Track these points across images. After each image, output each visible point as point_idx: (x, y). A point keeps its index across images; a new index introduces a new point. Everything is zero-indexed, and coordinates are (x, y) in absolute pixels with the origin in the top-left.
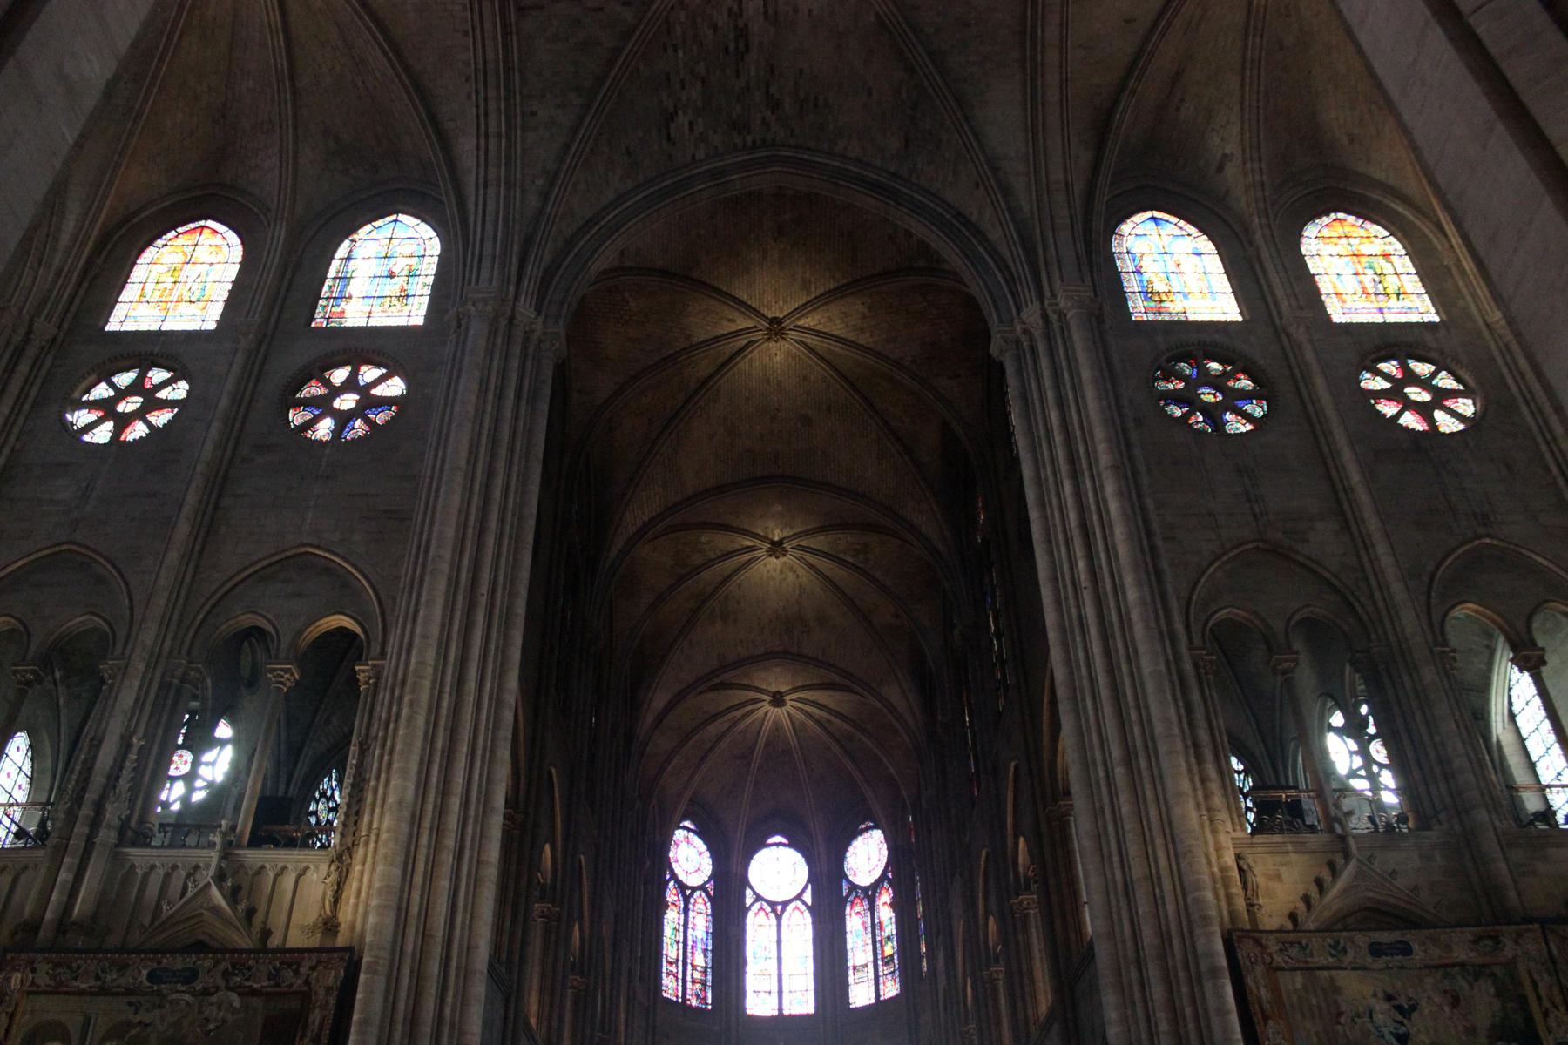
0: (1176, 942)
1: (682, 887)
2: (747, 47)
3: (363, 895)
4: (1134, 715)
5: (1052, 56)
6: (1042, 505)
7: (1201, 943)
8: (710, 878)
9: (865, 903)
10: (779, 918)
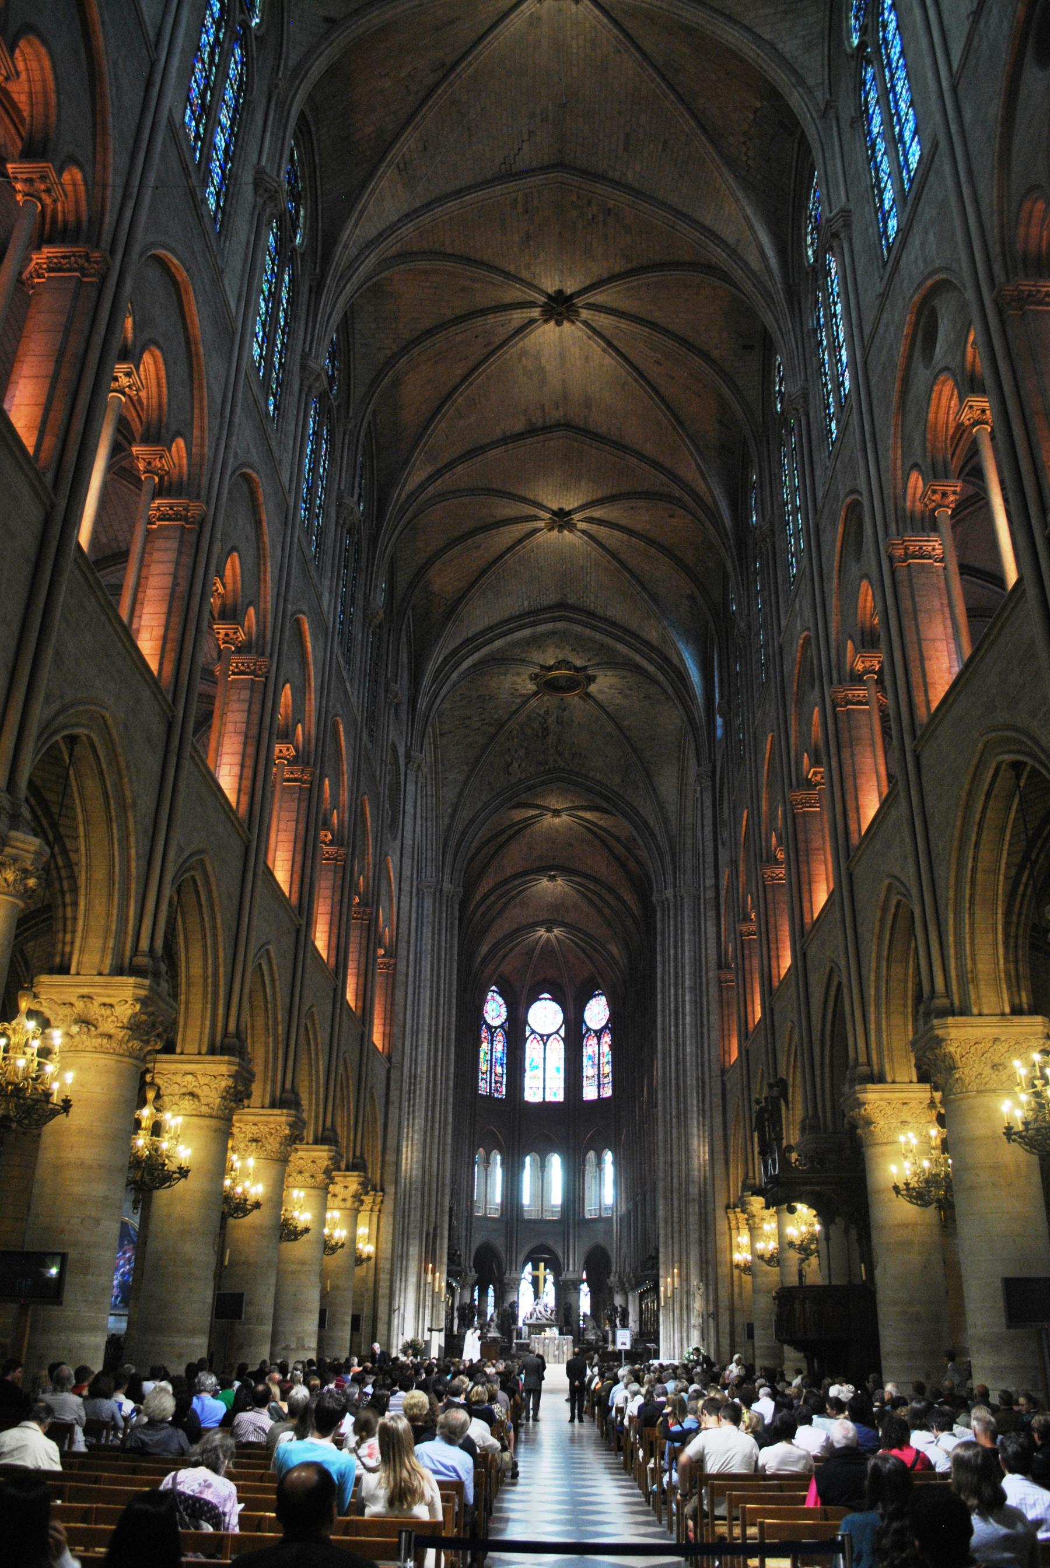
6: (663, 993)
10: (545, 1044)
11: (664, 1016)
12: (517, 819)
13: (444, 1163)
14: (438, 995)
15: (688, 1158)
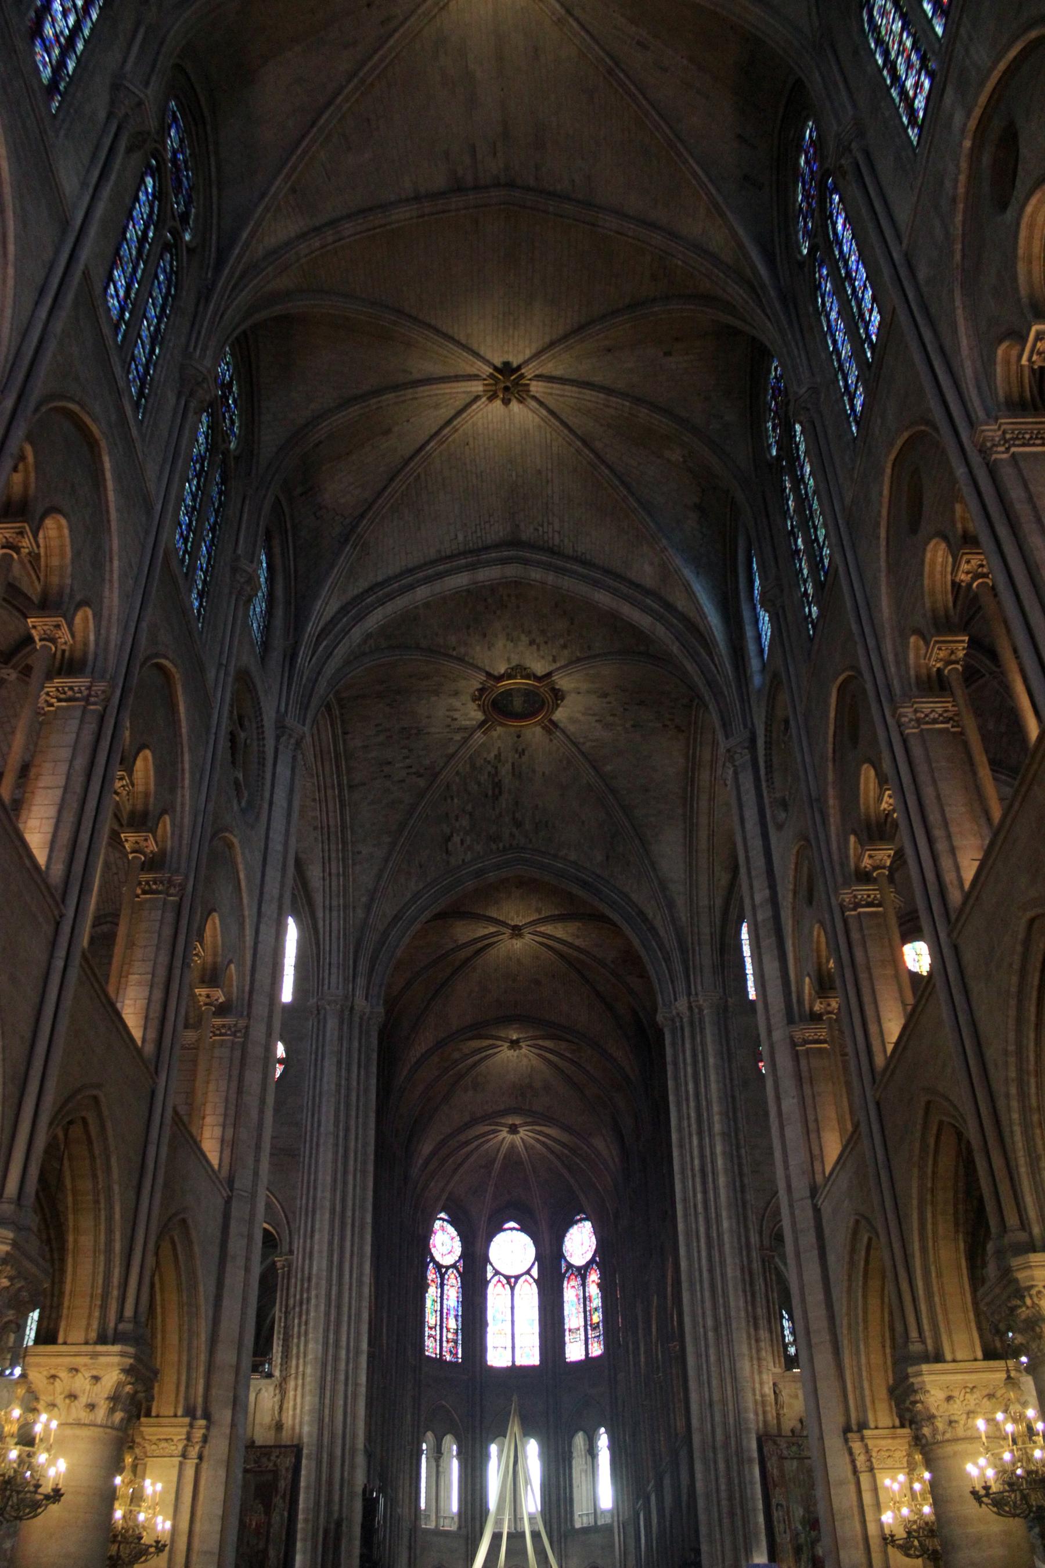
0: (733, 1440)
1: (438, 1266)
2: (500, 793)
3: (298, 1411)
4: (721, 1301)
5: (703, 820)
6: (681, 1146)
7: (745, 1443)
8: (460, 1258)
9: (579, 1279)
10: (512, 1289)
11: (684, 1181)
12: (463, 939)
13: (354, 1417)
14: (346, 1156)
15: (737, 1391)
